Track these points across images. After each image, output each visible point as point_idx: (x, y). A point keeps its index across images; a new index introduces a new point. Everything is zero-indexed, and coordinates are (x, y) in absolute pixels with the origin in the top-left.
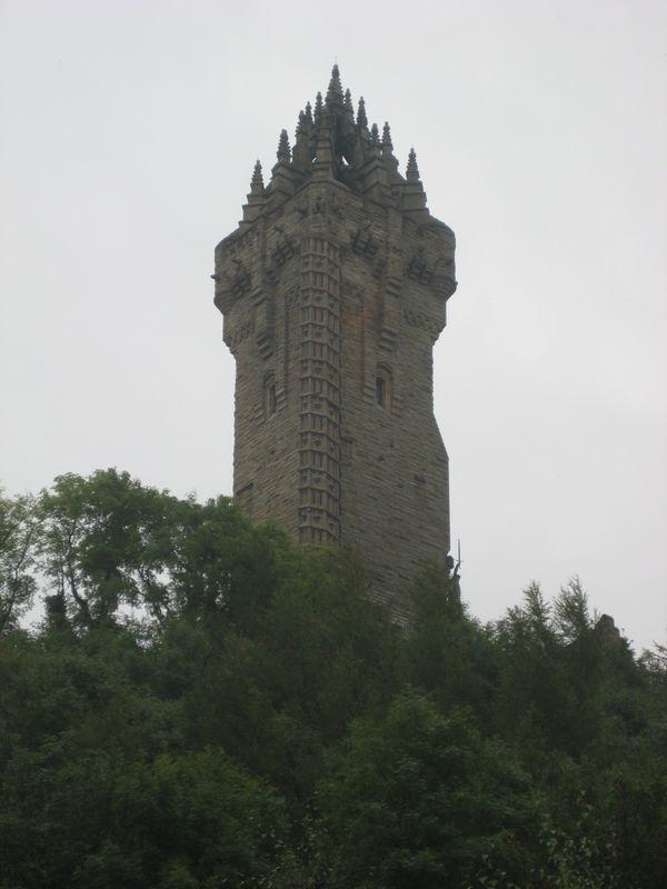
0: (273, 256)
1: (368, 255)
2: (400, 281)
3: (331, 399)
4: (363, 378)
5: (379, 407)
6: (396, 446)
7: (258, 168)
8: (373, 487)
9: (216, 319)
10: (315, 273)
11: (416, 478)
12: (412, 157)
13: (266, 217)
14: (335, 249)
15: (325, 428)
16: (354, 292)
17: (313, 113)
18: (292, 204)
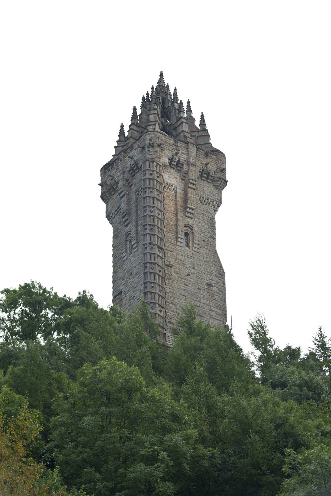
0: (129, 171)
1: (178, 168)
2: (196, 181)
3: (159, 244)
4: (177, 233)
5: (187, 248)
6: (196, 268)
7: (122, 127)
8: (184, 290)
9: (102, 206)
10: (149, 179)
11: (208, 284)
12: (202, 116)
13: (125, 151)
14: (160, 166)
15: (156, 261)
16: (172, 188)
17: (150, 97)
18: (137, 143)
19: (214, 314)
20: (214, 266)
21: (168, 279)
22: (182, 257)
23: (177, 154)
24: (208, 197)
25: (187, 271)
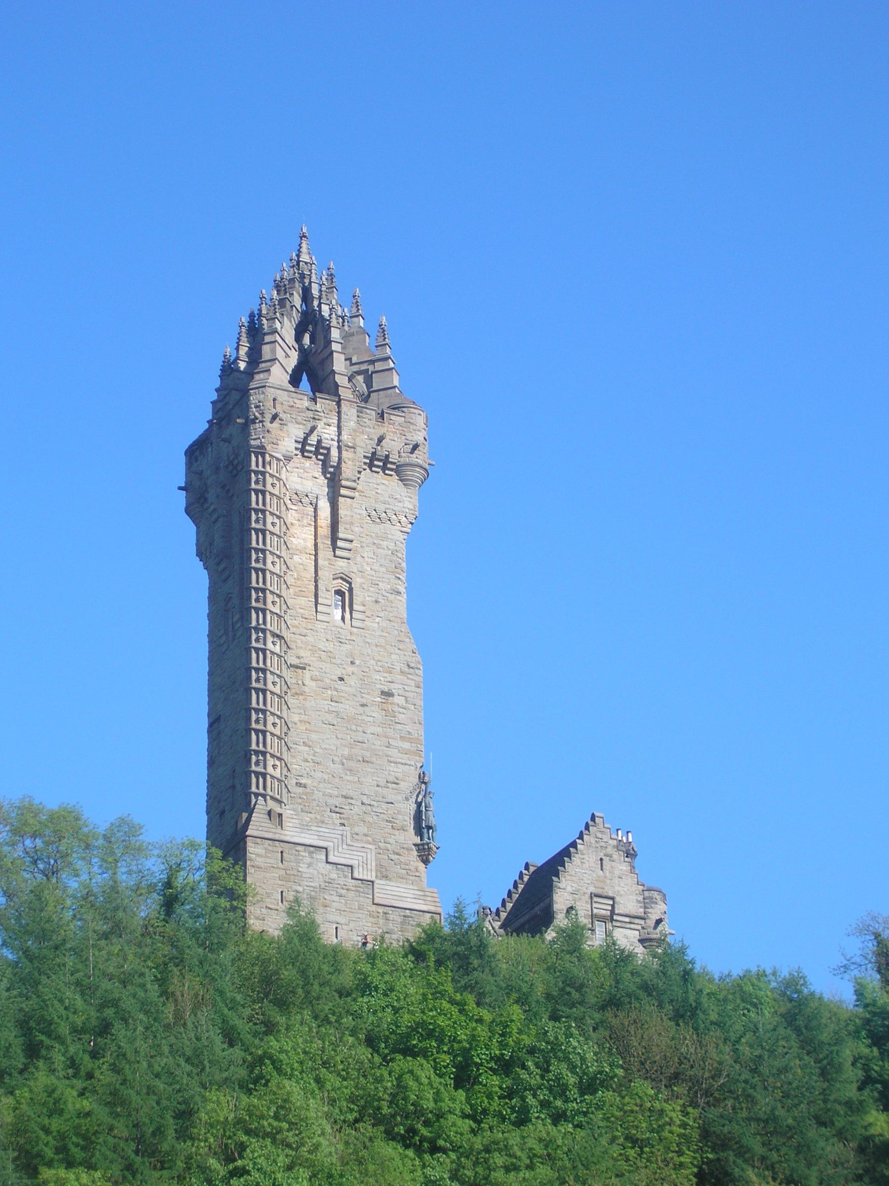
0: (227, 467)
6: (357, 662)
8: (330, 712)
11: (383, 693)
14: (278, 460)
16: (305, 500)
19: (394, 752)
20: (398, 651)
21: (296, 694)
22: (327, 645)
23: (313, 429)
24: (388, 506)
25: (339, 672)
